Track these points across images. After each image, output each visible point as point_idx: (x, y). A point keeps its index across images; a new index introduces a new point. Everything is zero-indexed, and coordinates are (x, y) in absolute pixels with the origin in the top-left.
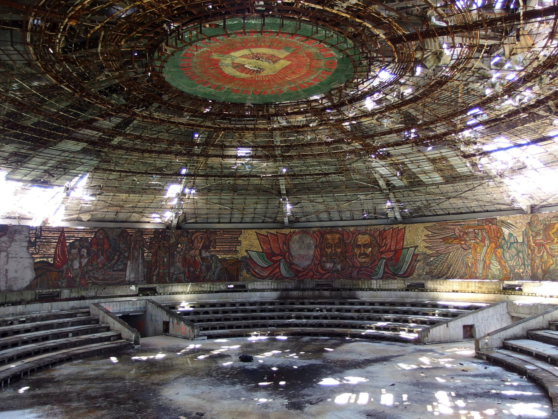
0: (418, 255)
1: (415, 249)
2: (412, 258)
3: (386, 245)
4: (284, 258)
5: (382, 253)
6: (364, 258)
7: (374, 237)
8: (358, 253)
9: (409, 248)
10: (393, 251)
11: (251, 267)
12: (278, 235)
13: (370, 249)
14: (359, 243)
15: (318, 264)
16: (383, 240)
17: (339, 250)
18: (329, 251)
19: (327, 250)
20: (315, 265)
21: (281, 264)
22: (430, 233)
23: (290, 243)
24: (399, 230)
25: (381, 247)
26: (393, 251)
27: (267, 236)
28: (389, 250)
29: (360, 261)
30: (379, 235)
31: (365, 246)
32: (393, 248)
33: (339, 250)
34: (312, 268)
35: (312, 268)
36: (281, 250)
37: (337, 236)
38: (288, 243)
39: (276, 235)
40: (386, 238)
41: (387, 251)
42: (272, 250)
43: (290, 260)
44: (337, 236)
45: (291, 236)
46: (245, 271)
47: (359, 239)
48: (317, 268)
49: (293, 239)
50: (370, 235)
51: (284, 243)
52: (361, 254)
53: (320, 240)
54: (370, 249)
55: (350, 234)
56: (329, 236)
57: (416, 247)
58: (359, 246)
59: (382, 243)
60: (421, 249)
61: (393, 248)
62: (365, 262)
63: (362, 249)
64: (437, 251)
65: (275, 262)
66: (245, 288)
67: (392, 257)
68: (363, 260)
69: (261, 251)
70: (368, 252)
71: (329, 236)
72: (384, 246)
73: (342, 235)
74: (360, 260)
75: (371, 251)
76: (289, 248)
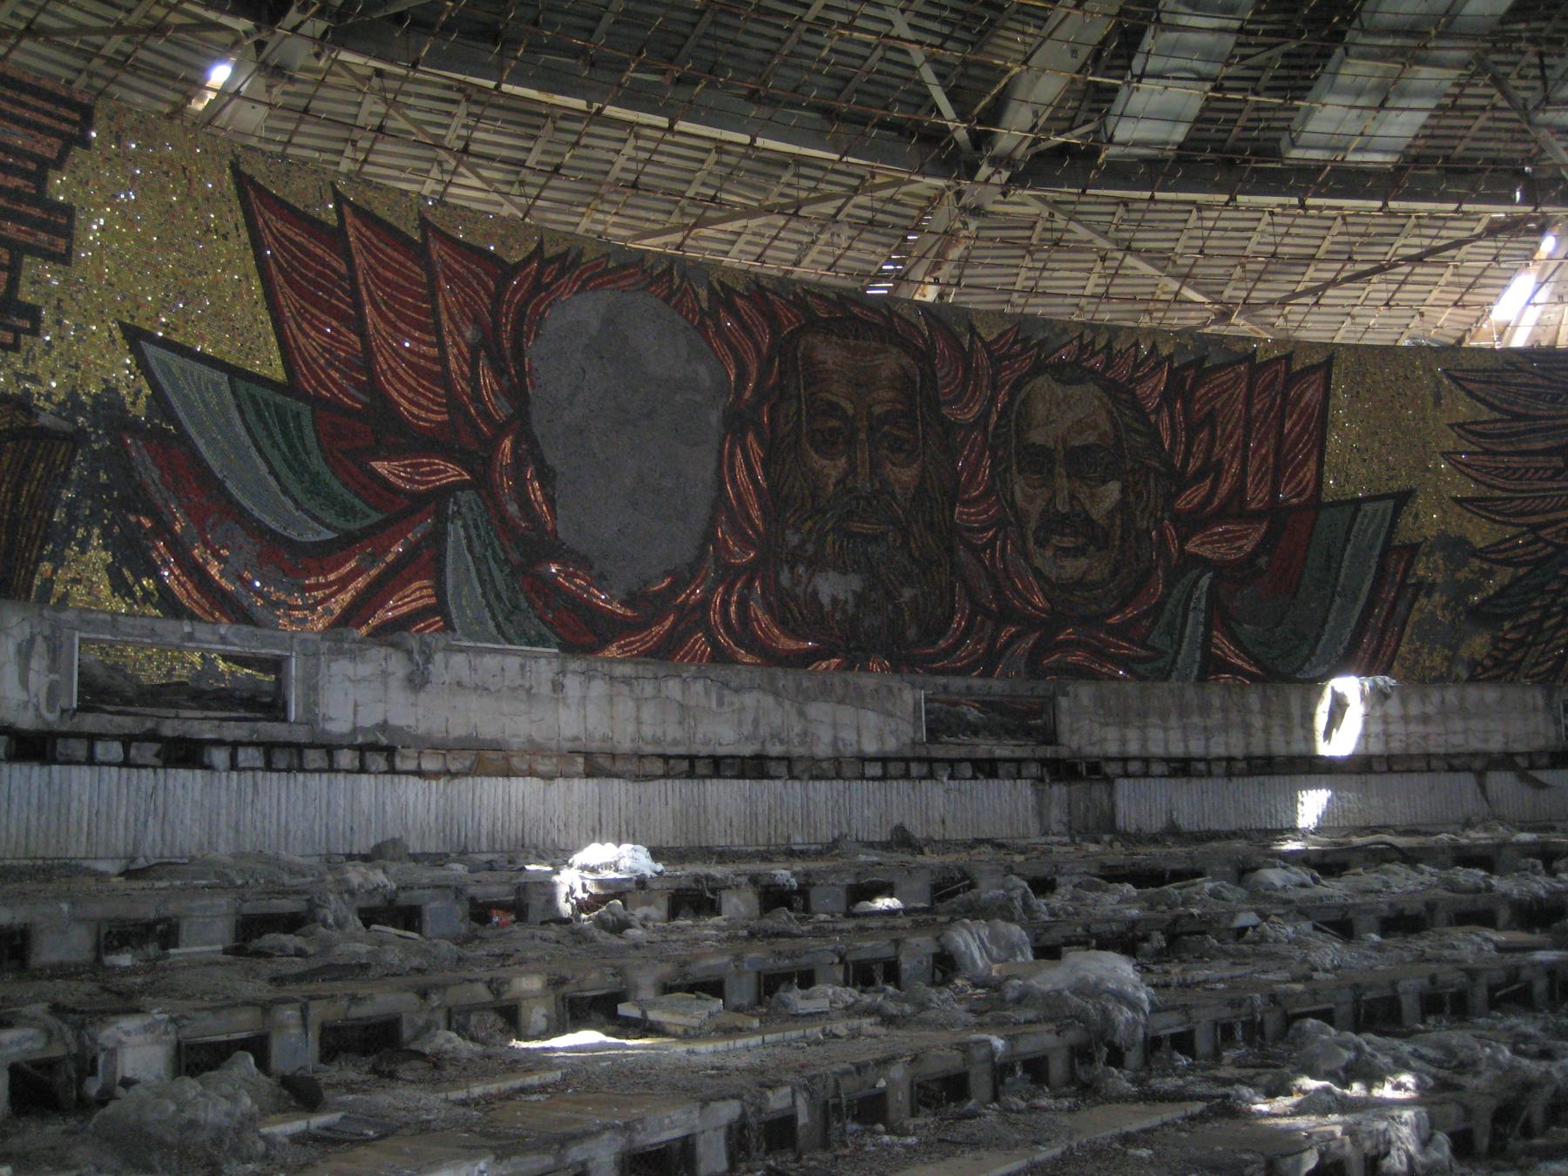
0: (1412, 550)
1: (1396, 512)
2: (1382, 568)
3: (1212, 469)
4: (482, 482)
5: (1193, 523)
6: (1078, 552)
7: (1137, 405)
8: (1035, 509)
9: (1357, 503)
10: (1256, 516)
11: (162, 527)
12: (436, 248)
13: (1113, 490)
14: (1037, 437)
15: (751, 571)
16: (1192, 431)
17: (904, 475)
18: (832, 469)
19: (818, 461)
20: (728, 574)
21: (455, 533)
22: (1486, 414)
23: (534, 350)
24: (1292, 378)
25: (1182, 482)
26: (1256, 516)
27: (335, 237)
28: (1235, 509)
29: (1051, 572)
30: (1167, 398)
31: (1081, 461)
32: (1257, 497)
33: (904, 475)
34: (704, 604)
35: (704, 604)
36: (454, 404)
37: (890, 362)
38: (519, 352)
39: (419, 252)
40: (1210, 419)
41: (1220, 516)
42: (373, 387)
43: (525, 504)
44: (890, 362)
45: (537, 286)
46: (99, 556)
47: (1040, 410)
48: (743, 605)
49: (555, 320)
50: (1112, 389)
51: (488, 346)
52: (1053, 523)
53: (763, 373)
54: (1113, 490)
55: (982, 358)
56: (829, 354)
57: (1403, 499)
58: (1038, 461)
59: (1188, 453)
60: (1428, 519)
61: (1257, 497)
62: (1080, 583)
63: (1062, 482)
64: (1534, 528)
65: (400, 508)
66: (275, 708)
67: (1255, 553)
68: (1072, 568)
69: (280, 375)
70: (1098, 512)
71: (829, 354)
72: (1200, 475)
73: (925, 357)
74: (1043, 559)
75: (1122, 506)
76: (518, 395)
